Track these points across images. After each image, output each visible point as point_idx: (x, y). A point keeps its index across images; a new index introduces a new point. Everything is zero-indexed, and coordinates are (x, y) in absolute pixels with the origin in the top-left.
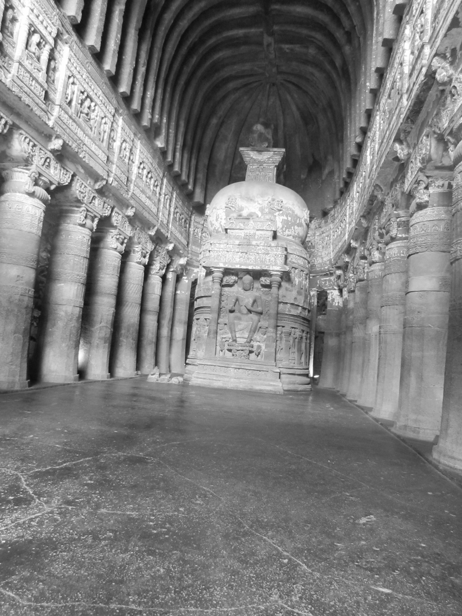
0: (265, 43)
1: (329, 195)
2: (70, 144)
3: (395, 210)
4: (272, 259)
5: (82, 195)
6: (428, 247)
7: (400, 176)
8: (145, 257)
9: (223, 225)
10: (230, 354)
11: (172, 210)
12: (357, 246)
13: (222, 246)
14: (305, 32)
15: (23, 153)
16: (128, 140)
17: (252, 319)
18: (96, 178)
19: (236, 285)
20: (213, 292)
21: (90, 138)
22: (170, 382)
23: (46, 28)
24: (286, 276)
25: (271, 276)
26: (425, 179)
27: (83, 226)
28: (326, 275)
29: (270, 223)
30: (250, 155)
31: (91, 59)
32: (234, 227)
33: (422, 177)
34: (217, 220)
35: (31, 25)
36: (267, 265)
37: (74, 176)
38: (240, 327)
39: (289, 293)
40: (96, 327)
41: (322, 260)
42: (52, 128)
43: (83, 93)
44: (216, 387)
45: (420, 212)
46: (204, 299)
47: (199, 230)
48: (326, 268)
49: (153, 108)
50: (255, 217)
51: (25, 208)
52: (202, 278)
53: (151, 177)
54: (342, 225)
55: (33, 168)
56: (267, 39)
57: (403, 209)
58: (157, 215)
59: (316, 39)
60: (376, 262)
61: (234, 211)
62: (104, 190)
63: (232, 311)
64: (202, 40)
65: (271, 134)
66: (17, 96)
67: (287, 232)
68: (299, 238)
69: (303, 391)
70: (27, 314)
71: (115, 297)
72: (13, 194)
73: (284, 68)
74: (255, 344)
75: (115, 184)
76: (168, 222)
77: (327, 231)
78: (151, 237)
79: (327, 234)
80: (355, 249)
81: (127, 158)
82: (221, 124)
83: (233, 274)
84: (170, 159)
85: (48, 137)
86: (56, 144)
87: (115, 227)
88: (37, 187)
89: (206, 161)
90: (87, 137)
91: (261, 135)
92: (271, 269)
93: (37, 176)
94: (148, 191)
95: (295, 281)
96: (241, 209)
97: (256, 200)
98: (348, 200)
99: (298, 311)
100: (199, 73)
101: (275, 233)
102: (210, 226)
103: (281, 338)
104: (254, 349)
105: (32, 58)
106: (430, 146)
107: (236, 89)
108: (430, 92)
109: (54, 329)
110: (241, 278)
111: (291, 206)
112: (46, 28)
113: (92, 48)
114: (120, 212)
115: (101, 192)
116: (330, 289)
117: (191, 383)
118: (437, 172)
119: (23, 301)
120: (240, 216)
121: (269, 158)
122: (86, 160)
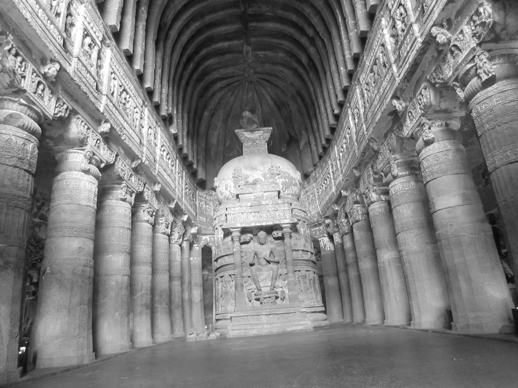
0: (245, 52)
1: (308, 161)
2: (115, 128)
4: (282, 214)
6: (444, 172)
7: (396, 126)
8: (167, 228)
10: (259, 303)
11: (184, 186)
12: (347, 194)
13: (237, 209)
14: (276, 41)
15: (80, 135)
16: (152, 127)
17: (272, 269)
19: (252, 241)
20: (235, 250)
21: (128, 124)
22: (209, 338)
23: (95, 32)
24: (294, 227)
25: (282, 229)
26: (427, 121)
27: (124, 200)
28: (315, 226)
30: (244, 135)
31: (125, 60)
32: (244, 192)
33: (424, 120)
34: (226, 189)
35: (85, 30)
37: (117, 156)
39: (299, 241)
40: (137, 295)
41: (311, 214)
42: (103, 113)
43: (120, 86)
44: (252, 335)
45: (428, 147)
47: (203, 203)
48: (315, 219)
49: (168, 101)
50: (260, 182)
51: (82, 184)
52: (220, 240)
53: (169, 159)
54: (326, 182)
55: (88, 148)
56: (247, 48)
57: (398, 153)
59: (286, 46)
60: (375, 202)
61: (241, 180)
62: (138, 169)
63: (252, 265)
64: (196, 52)
65: (257, 118)
66: (78, 84)
67: (287, 192)
68: (296, 195)
69: (325, 326)
70: (90, 284)
71: (151, 265)
72: (69, 172)
73: (258, 70)
74: (279, 290)
75: (147, 163)
76: (182, 197)
78: (171, 209)
79: (311, 192)
80: (346, 197)
82: (213, 115)
84: (180, 143)
85: (99, 122)
86: (105, 127)
87: (146, 202)
88: (91, 165)
89: (203, 145)
90: (125, 123)
91: (249, 119)
92: (282, 222)
93: (91, 155)
94: (168, 170)
96: (247, 177)
97: (258, 168)
98: (329, 161)
99: (308, 256)
100: (195, 77)
101: (279, 192)
102: (220, 195)
103: (299, 281)
104: (279, 295)
105: (86, 56)
106: (430, 94)
107: (222, 88)
108: (426, 55)
109: (106, 300)
110: (257, 235)
111: (287, 171)
112: (95, 32)
113: (126, 52)
115: (136, 170)
116: (321, 237)
117: (228, 336)
118: (435, 115)
119: (86, 271)
120: (247, 182)
121: (260, 136)
122: (127, 142)
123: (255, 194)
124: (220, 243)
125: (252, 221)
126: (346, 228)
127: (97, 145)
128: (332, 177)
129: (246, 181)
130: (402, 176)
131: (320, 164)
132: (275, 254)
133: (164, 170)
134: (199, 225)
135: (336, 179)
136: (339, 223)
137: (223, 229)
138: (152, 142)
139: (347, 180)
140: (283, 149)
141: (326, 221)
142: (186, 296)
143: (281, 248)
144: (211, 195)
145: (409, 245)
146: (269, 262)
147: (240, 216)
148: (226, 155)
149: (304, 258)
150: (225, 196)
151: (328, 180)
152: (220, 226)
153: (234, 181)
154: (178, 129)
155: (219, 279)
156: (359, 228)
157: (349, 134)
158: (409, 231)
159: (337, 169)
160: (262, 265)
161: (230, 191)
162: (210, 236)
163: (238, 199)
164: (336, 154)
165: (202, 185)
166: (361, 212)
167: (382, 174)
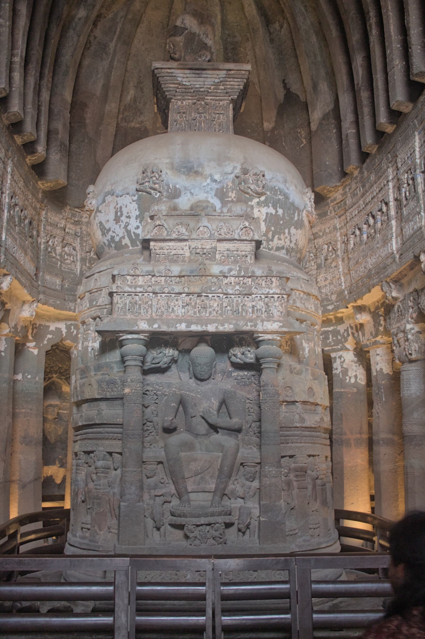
4: (260, 305)
9: (133, 230)
10: (179, 533)
11: (7, 200)
13: (140, 281)
17: (221, 447)
19: (174, 367)
20: (127, 390)
25: (257, 343)
29: (247, 224)
32: (164, 235)
36: (251, 320)
38: (193, 466)
46: (103, 405)
47: (57, 241)
52: (91, 355)
54: (371, 221)
63: (169, 431)
65: (211, 36)
67: (276, 242)
77: (325, 233)
83: (167, 344)
91: (192, 37)
92: (260, 328)
95: (304, 349)
96: (175, 194)
97: (207, 171)
98: (390, 170)
103: (289, 484)
110: (188, 351)
120: (175, 208)
123: (193, 244)
124: (91, 364)
125: (181, 317)
128: (393, 212)
132: (232, 409)
135: (408, 220)
141: (358, 316)
143: (247, 394)
144: (77, 223)
146: (215, 428)
148: (124, 124)
149: (308, 424)
150: (113, 237)
151: (379, 217)
153: (139, 201)
155: (82, 456)
160: (197, 435)
161: (126, 227)
162: (69, 323)
163: (146, 253)
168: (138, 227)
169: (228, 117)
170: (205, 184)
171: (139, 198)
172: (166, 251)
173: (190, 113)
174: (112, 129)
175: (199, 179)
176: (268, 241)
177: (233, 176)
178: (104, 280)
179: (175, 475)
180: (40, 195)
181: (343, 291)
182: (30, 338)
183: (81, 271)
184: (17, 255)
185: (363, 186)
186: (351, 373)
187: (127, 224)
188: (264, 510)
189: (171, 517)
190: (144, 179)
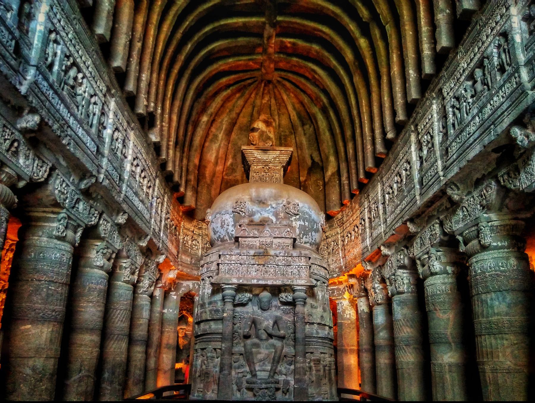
3: (485, 213)
5: (62, 196)
11: (164, 216)
12: (389, 253)
18: (84, 174)
37: (52, 169)
40: (73, 379)
47: (189, 238)
48: (335, 276)
50: (270, 223)
53: (145, 177)
54: (356, 229)
58: (149, 223)
60: (436, 274)
67: (304, 239)
75: (106, 183)
76: (160, 230)
78: (141, 249)
80: (386, 256)
81: (119, 151)
87: (102, 239)
94: (141, 193)
96: (252, 214)
97: (269, 203)
101: (295, 240)
111: (308, 210)
114: (109, 220)
115: (87, 194)
120: (252, 221)
121: (275, 158)
123: (261, 239)
126: (380, 296)
127: (13, 149)
128: (367, 225)
129: (250, 219)
130: (496, 248)
131: (351, 204)
133: (134, 193)
134: (180, 267)
135: (375, 229)
136: (369, 288)
137: (212, 284)
138: (119, 151)
139: (393, 234)
140: (301, 178)
141: (350, 280)
142: (152, 363)
144: (200, 228)
145: (498, 357)
147: (236, 268)
148: (226, 177)
150: (219, 236)
151: (360, 227)
152: (209, 277)
154: (161, 136)
156: (402, 303)
157: (406, 170)
158: (500, 336)
159: (378, 216)
163: (237, 244)
164: (379, 195)
165: (190, 214)
166: (408, 281)
167: (460, 238)
168: (233, 231)
169: (280, 175)
170: (268, 209)
171: (234, 216)
172: (247, 243)
173: (261, 173)
174: (219, 180)
175: (265, 206)
176: (300, 238)
177: (282, 205)
178: (214, 257)
179: (250, 361)
180: (181, 214)
181: (342, 267)
182: (173, 289)
183: (202, 254)
184: (168, 244)
185: (352, 211)
186: (347, 312)
187: (228, 229)
188: (297, 381)
189: (246, 384)
190: (236, 206)
